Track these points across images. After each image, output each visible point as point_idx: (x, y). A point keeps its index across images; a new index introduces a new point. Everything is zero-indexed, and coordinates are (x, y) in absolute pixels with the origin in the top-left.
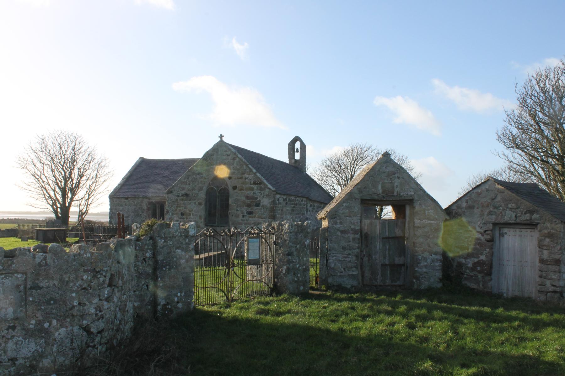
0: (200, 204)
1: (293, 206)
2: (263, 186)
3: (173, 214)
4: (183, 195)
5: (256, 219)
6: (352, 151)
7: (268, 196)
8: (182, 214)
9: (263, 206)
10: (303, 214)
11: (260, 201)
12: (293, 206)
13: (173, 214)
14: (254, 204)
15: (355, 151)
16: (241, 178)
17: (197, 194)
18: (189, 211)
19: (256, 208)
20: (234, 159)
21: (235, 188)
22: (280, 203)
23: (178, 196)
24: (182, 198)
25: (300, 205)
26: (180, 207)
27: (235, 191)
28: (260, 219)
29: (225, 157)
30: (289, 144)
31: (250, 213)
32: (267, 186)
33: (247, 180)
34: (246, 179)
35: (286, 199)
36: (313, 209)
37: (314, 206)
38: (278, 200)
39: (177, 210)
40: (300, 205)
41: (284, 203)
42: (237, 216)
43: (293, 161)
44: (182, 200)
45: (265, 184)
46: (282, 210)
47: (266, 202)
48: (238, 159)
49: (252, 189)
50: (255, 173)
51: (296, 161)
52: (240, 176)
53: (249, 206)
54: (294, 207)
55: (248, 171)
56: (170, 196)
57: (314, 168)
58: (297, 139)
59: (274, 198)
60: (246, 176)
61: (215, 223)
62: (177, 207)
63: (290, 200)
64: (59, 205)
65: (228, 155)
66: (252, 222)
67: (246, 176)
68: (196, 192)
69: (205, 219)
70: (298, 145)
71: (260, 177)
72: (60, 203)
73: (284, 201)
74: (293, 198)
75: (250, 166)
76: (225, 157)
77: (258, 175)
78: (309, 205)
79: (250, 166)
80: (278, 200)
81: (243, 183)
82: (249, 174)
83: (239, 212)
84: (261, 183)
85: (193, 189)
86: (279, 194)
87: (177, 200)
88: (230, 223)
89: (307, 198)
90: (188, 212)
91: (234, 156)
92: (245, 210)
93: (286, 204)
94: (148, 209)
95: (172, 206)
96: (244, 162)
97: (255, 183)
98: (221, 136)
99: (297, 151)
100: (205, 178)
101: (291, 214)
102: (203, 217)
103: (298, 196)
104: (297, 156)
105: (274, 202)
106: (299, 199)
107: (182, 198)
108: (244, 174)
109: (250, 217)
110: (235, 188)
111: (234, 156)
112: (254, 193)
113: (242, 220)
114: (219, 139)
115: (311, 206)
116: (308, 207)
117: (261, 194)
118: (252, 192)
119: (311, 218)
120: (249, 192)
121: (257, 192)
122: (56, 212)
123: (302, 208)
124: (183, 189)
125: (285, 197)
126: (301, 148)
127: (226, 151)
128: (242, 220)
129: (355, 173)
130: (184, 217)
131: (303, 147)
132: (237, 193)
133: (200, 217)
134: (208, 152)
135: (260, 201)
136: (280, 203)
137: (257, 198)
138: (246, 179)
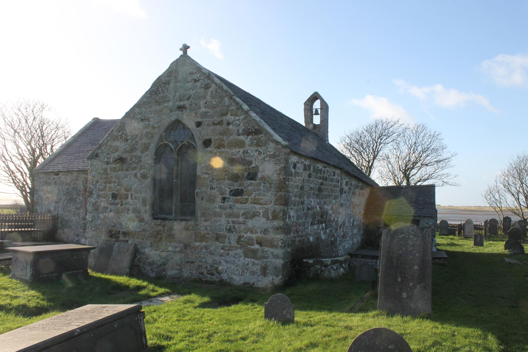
0: (144, 176)
1: (320, 181)
2: (262, 137)
3: (99, 196)
4: (115, 161)
5: (248, 206)
6: (376, 126)
7: (273, 156)
8: (114, 196)
9: (263, 179)
11: (257, 167)
12: (320, 181)
13: (99, 196)
15: (380, 126)
16: (220, 123)
17: (140, 157)
18: (126, 190)
19: (249, 182)
20: (207, 87)
21: (207, 143)
22: (297, 174)
23: (108, 163)
24: (114, 166)
25: (332, 180)
26: (110, 183)
27: (209, 149)
28: (257, 206)
29: (189, 85)
30: (305, 104)
31: (237, 193)
32: (271, 136)
33: (231, 127)
36: (350, 189)
37: (351, 185)
38: (294, 167)
39: (105, 187)
40: (332, 180)
41: (305, 175)
43: (311, 127)
44: (114, 170)
45: (267, 133)
46: (302, 188)
47: (269, 169)
48: (213, 86)
49: (241, 144)
50: (247, 112)
51: (315, 126)
52: (217, 119)
54: (322, 184)
55: (234, 108)
56: (95, 162)
57: (337, 138)
58: (315, 97)
59: (287, 161)
60: (229, 117)
61: (171, 214)
62: (106, 183)
63: (317, 171)
64: (28, 190)
65: (196, 81)
66: (242, 212)
67: (229, 117)
68: (138, 153)
69: (153, 205)
70: (317, 105)
71: (258, 119)
72: (29, 187)
73: (305, 169)
74: (320, 166)
75: (238, 100)
76: (189, 85)
77: (253, 115)
78: (344, 182)
79: (238, 100)
80: (294, 167)
81: (223, 133)
83: (215, 192)
84: (258, 131)
85: (133, 149)
86: (296, 153)
87: (106, 170)
88: (199, 213)
89: (341, 169)
90: (123, 191)
91: (207, 81)
92: (227, 187)
93: (310, 176)
95: (97, 182)
97: (247, 133)
99: (317, 113)
100: (154, 127)
101: (318, 196)
102: (149, 201)
103: (329, 164)
104: (317, 120)
105: (285, 170)
106: (331, 170)
107: (114, 166)
108: (226, 114)
111: (207, 81)
115: (347, 183)
116: (344, 186)
117: (260, 153)
118: (241, 150)
120: (235, 150)
121: (252, 151)
122: (25, 197)
125: (307, 163)
126: (321, 109)
127: (192, 74)
128: (220, 207)
129: (378, 152)
130: (117, 201)
131: (325, 107)
133: (144, 203)
134: (159, 79)
135: (257, 167)
137: (251, 163)
138: (229, 124)
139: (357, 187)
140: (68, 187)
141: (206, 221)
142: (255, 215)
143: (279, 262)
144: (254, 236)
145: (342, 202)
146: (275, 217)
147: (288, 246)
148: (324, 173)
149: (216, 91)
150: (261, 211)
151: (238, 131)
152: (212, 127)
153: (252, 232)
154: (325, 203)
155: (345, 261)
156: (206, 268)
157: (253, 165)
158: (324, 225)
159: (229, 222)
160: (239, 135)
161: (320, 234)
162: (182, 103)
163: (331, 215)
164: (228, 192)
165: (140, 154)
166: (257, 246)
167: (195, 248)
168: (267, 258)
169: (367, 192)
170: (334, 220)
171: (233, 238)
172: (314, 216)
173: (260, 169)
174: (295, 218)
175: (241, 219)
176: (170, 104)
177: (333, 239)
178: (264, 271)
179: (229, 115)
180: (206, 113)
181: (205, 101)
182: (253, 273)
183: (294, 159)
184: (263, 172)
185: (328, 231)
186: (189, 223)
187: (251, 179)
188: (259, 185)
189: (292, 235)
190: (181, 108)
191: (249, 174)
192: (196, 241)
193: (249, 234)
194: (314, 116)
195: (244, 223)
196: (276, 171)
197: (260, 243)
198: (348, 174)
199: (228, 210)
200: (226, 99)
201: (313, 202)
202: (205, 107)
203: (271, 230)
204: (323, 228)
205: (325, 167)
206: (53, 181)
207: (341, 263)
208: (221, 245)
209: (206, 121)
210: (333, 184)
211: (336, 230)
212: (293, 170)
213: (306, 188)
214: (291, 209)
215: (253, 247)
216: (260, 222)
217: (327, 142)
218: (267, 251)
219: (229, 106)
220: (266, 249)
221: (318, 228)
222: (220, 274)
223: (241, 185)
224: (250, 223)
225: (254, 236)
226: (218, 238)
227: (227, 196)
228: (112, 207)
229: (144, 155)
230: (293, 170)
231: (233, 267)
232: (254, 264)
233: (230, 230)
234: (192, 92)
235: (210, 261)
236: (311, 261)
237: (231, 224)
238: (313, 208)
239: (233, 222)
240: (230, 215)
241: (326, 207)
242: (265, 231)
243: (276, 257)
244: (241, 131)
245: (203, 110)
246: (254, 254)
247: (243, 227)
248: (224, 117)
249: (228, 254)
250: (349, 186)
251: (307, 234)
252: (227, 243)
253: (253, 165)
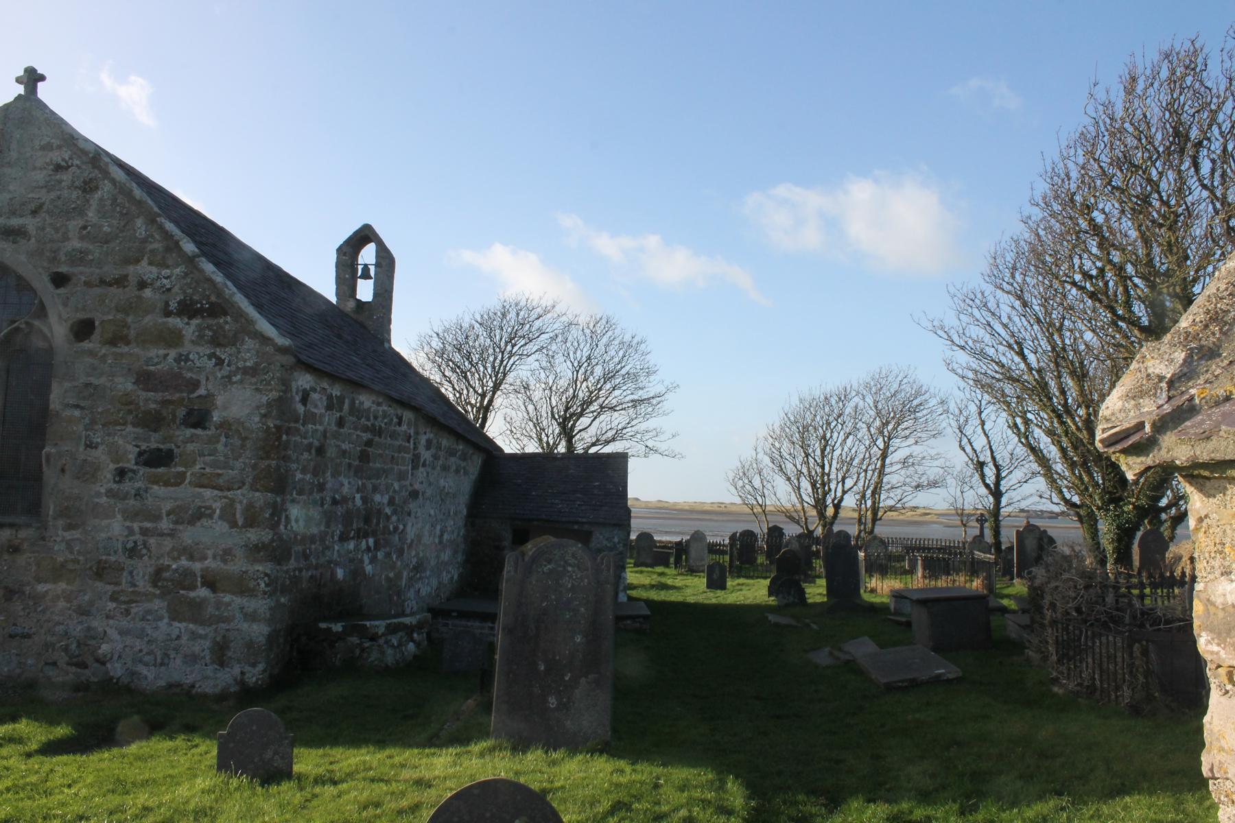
1: (366, 436)
2: (228, 324)
5: (185, 492)
6: (504, 315)
9: (225, 425)
10: (401, 477)
12: (366, 436)
14: (181, 412)
15: (512, 315)
16: (120, 282)
19: (189, 432)
20: (88, 187)
25: (393, 435)
27: (86, 345)
28: (208, 493)
30: (339, 250)
31: (157, 459)
32: (251, 322)
33: (148, 293)
34: (142, 285)
35: (341, 400)
36: (436, 457)
37: (439, 448)
38: (305, 400)
40: (393, 435)
41: (329, 419)
42: (88, 473)
43: (351, 305)
45: (240, 315)
46: (320, 451)
47: (239, 404)
48: (107, 186)
49: (172, 339)
50: (191, 260)
52: (112, 271)
53: (152, 421)
54: (369, 443)
57: (411, 336)
58: (364, 236)
59: (286, 384)
60: (145, 269)
65: (58, 168)
66: (167, 506)
70: (368, 255)
73: (329, 407)
75: (170, 226)
77: (209, 268)
78: (423, 440)
79: (170, 226)
80: (305, 400)
82: (163, 265)
83: (100, 454)
84: (219, 309)
86: (310, 368)
88: (51, 507)
89: (415, 409)
92: (129, 442)
93: (341, 423)
96: (140, 203)
97: (188, 309)
98: (32, 78)
99: (366, 275)
101: (358, 472)
104: (365, 291)
105: (281, 406)
106: (391, 411)
108: (137, 261)
109: (156, 480)
113: (110, 493)
114: (21, 89)
115: (429, 442)
116: (421, 449)
117: (220, 362)
118: (173, 353)
119: (429, 492)
120: (155, 352)
121: (200, 356)
123: (401, 449)
125: (336, 391)
126: (377, 265)
127: (47, 147)
128: (110, 493)
129: (505, 375)
131: (386, 261)
132: (91, 353)
135: (210, 397)
136: (310, 418)
137: (195, 385)
138: (142, 285)
139: (452, 453)
141: (70, 527)
142: (199, 515)
143: (259, 631)
144: (197, 566)
145: (417, 486)
146: (251, 522)
147: (282, 592)
148: (376, 418)
149: (114, 200)
150: (217, 506)
151: (167, 304)
152: (98, 290)
153: (191, 558)
154: (375, 489)
155: (419, 626)
156: (66, 649)
157: (202, 391)
158: (371, 541)
159: (131, 531)
160: (168, 314)
161: (362, 561)
162: (15, 222)
163: (388, 518)
164: (132, 457)
166: (203, 592)
167: (37, 598)
168: (227, 620)
169: (475, 465)
170: (396, 529)
172: (348, 518)
173: (220, 400)
174: (301, 523)
175: (165, 525)
177: (391, 575)
178: (220, 654)
179: (144, 263)
180: (83, 252)
181: (81, 223)
182: (192, 659)
183: (304, 380)
184: (225, 408)
185: (380, 555)
186: (23, 534)
187: (195, 426)
188: (214, 440)
189: (292, 564)
191: (190, 413)
192: (39, 580)
193: (184, 562)
195: (172, 534)
196: (258, 407)
198: (432, 421)
199: (132, 502)
200: (139, 222)
201: (347, 485)
202: (82, 238)
203: (239, 553)
204: (368, 549)
205: (379, 404)
207: (409, 630)
208: (110, 588)
209: (82, 273)
210: (397, 443)
211: (401, 552)
212: (301, 409)
213: (331, 452)
214: (293, 501)
215: (192, 594)
216: (213, 533)
217: (386, 345)
218: (229, 604)
219: (144, 241)
220: (227, 598)
221: (357, 547)
222: (104, 663)
224: (188, 535)
225: (197, 566)
226: (101, 571)
227: (131, 465)
230: (301, 409)
231: (138, 644)
232: (194, 636)
233: (132, 552)
234: (46, 197)
235: (77, 630)
236: (338, 627)
237: (137, 537)
238: (345, 500)
239: (144, 532)
240: (137, 514)
241: (377, 498)
242: (226, 555)
243: (252, 617)
244: (173, 305)
245: (77, 244)
246: (194, 611)
247: (168, 543)
248: (131, 268)
249: (127, 612)
250: (433, 451)
251: (330, 562)
252: (124, 585)
253: (202, 391)
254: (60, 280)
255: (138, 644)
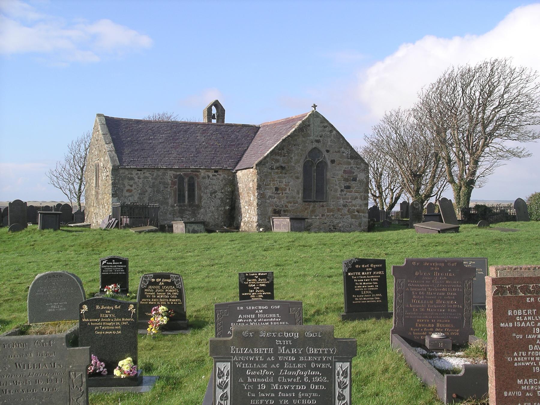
0: (297, 178)
4: (277, 168)
5: (353, 194)
8: (277, 189)
16: (339, 152)
28: (357, 194)
31: (348, 187)
33: (344, 154)
42: (336, 191)
49: (349, 163)
52: (337, 150)
53: (346, 180)
83: (337, 187)
87: (270, 173)
94: (174, 183)
97: (352, 158)
108: (341, 148)
110: (333, 162)
112: (351, 168)
124: (277, 161)
138: (343, 152)
140: (154, 181)
142: (356, 198)
153: (355, 207)
165: (294, 165)
166: (356, 213)
171: (345, 211)
173: (358, 176)
176: (311, 138)
190: (318, 141)
194: (227, 121)
195: (351, 202)
197: (358, 212)
203: (363, 205)
206: (137, 176)
223: (350, 183)
226: (339, 210)
228: (276, 196)
229: (297, 166)
242: (361, 206)
245: (329, 143)
254: (328, 151)
255: (346, 224)
